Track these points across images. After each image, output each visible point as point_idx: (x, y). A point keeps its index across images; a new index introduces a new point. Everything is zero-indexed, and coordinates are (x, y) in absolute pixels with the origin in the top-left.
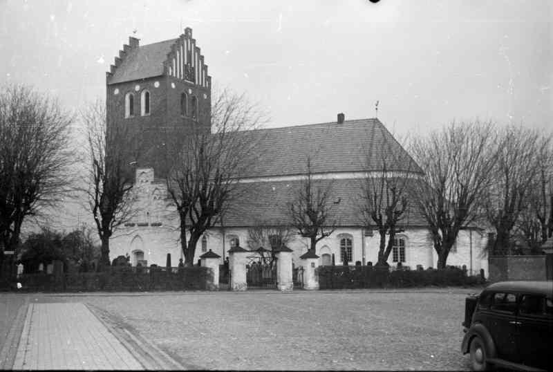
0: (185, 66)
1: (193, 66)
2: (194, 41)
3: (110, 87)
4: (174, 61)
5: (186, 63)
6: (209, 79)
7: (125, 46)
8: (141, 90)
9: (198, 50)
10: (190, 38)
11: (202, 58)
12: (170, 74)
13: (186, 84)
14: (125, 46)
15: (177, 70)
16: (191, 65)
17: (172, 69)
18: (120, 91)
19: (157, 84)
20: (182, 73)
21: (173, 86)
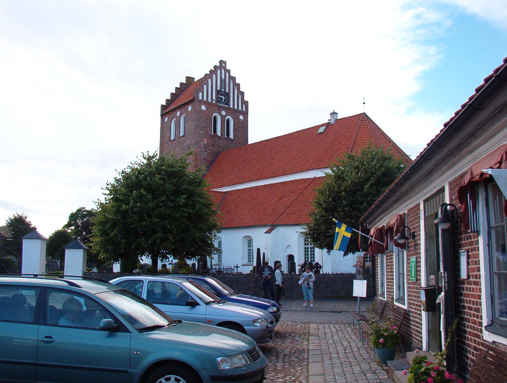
0: (218, 92)
1: (227, 91)
2: (229, 71)
3: (163, 116)
4: (205, 87)
5: (219, 89)
6: (246, 103)
7: (182, 84)
8: (181, 115)
9: (234, 79)
10: (225, 68)
11: (238, 86)
12: (200, 98)
13: (220, 107)
14: (182, 84)
15: (208, 94)
16: (225, 91)
17: (203, 94)
18: (168, 119)
19: (190, 108)
20: (214, 98)
21: (203, 108)
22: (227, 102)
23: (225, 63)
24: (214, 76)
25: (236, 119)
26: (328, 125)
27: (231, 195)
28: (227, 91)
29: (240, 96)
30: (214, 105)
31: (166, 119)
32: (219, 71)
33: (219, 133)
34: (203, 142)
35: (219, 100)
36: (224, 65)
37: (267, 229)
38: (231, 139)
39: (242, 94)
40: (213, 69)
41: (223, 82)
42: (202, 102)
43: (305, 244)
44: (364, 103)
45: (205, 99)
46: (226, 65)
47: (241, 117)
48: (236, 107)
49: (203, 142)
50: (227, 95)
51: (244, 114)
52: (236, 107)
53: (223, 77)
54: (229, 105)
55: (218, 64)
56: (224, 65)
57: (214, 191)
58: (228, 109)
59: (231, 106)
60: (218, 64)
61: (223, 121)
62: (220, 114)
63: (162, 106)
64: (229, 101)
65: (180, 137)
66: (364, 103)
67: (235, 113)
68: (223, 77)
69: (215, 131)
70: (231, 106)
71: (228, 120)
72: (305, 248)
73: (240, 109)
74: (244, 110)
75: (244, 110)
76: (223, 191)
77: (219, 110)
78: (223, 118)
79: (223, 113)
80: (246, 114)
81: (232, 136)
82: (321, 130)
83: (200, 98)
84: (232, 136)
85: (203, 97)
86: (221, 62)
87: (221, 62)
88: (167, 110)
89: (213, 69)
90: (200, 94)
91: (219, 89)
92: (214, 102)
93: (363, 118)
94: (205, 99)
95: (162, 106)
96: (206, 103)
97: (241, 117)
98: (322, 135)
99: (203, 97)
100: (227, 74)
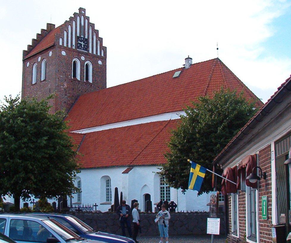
0: (78, 38)
1: (86, 37)
2: (88, 18)
3: (25, 61)
4: (65, 33)
5: (78, 35)
6: (104, 49)
7: (43, 30)
8: (42, 60)
9: (93, 25)
10: (84, 15)
11: (97, 32)
12: (61, 44)
13: (79, 52)
14: (43, 30)
15: (68, 40)
16: (84, 37)
17: (63, 40)
18: (30, 63)
19: (51, 54)
20: (74, 43)
21: (64, 53)
22: (86, 48)
23: (84, 10)
24: (74, 23)
25: (95, 64)
26: (183, 70)
27: (90, 137)
28: (86, 37)
29: (99, 42)
30: (74, 51)
31: (28, 64)
32: (78, 18)
33: (78, 78)
34: (63, 86)
35: (78, 46)
36: (83, 12)
37: (124, 169)
38: (90, 83)
39: (101, 40)
40: (73, 16)
41: (82, 28)
42: (62, 48)
43: (161, 184)
44: (218, 49)
45: (65, 45)
46: (85, 12)
47: (100, 62)
48: (95, 53)
49: (63, 86)
50: (86, 41)
51: (102, 59)
52: (95, 53)
53: (83, 24)
54: (88, 51)
55: (78, 12)
56: (83, 12)
57: (74, 133)
58: (87, 55)
59: (90, 52)
60: (78, 12)
61: (82, 66)
62: (80, 59)
63: (24, 51)
64: (88, 47)
65: (41, 82)
66: (218, 49)
67: (94, 58)
68: (83, 24)
69: (75, 76)
70: (90, 52)
71: (87, 65)
72: (161, 188)
73: (99, 54)
74: (102, 55)
75: (102, 55)
76: (83, 133)
77: (79, 55)
78: (82, 63)
79: (83, 58)
80: (104, 59)
81: (91, 81)
82: (177, 74)
83: (61, 44)
84: (91, 81)
85: (63, 43)
86: (81, 9)
87: (81, 9)
88: (29, 56)
89: (73, 16)
90: (61, 40)
91: (78, 35)
92: (74, 48)
93: (217, 63)
94: (65, 45)
95: (24, 51)
96: (66, 49)
97: (100, 62)
98: (177, 79)
99: (63, 43)
100: (86, 21)
